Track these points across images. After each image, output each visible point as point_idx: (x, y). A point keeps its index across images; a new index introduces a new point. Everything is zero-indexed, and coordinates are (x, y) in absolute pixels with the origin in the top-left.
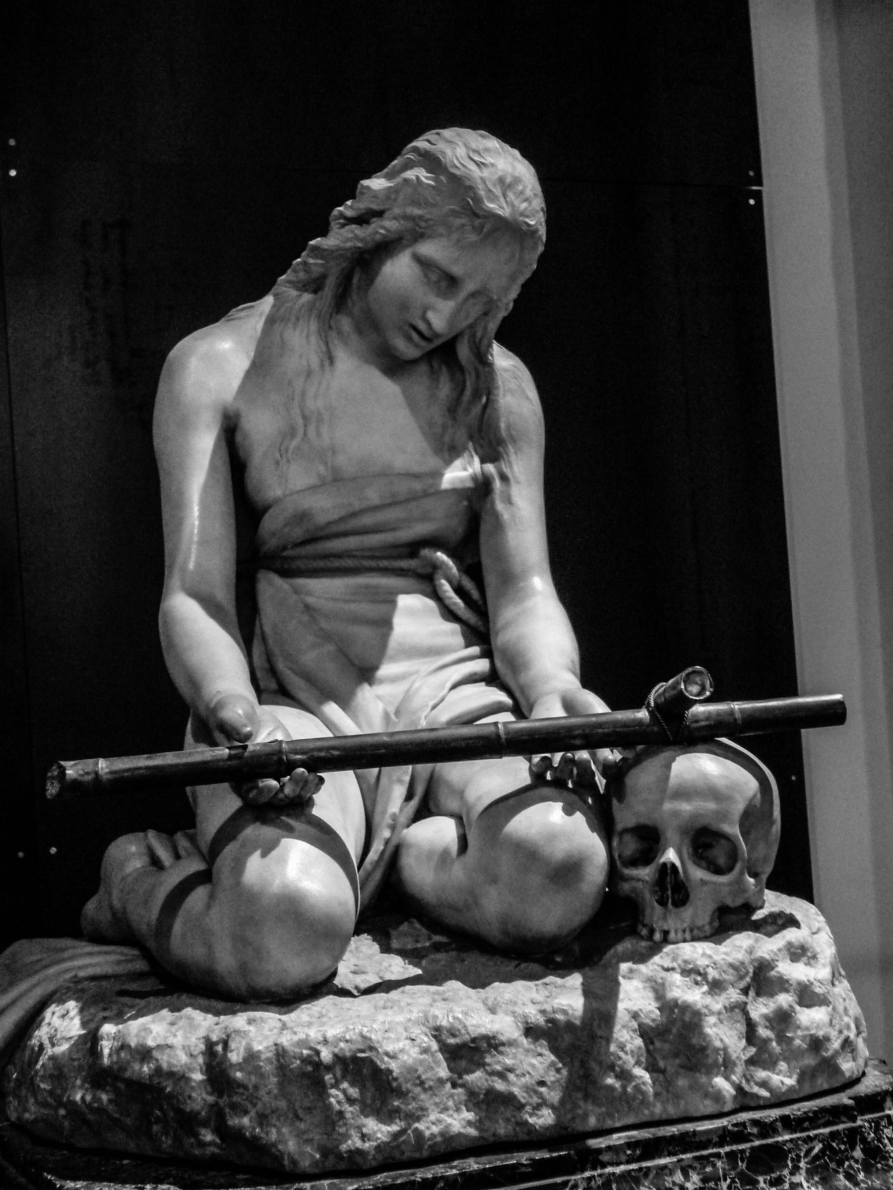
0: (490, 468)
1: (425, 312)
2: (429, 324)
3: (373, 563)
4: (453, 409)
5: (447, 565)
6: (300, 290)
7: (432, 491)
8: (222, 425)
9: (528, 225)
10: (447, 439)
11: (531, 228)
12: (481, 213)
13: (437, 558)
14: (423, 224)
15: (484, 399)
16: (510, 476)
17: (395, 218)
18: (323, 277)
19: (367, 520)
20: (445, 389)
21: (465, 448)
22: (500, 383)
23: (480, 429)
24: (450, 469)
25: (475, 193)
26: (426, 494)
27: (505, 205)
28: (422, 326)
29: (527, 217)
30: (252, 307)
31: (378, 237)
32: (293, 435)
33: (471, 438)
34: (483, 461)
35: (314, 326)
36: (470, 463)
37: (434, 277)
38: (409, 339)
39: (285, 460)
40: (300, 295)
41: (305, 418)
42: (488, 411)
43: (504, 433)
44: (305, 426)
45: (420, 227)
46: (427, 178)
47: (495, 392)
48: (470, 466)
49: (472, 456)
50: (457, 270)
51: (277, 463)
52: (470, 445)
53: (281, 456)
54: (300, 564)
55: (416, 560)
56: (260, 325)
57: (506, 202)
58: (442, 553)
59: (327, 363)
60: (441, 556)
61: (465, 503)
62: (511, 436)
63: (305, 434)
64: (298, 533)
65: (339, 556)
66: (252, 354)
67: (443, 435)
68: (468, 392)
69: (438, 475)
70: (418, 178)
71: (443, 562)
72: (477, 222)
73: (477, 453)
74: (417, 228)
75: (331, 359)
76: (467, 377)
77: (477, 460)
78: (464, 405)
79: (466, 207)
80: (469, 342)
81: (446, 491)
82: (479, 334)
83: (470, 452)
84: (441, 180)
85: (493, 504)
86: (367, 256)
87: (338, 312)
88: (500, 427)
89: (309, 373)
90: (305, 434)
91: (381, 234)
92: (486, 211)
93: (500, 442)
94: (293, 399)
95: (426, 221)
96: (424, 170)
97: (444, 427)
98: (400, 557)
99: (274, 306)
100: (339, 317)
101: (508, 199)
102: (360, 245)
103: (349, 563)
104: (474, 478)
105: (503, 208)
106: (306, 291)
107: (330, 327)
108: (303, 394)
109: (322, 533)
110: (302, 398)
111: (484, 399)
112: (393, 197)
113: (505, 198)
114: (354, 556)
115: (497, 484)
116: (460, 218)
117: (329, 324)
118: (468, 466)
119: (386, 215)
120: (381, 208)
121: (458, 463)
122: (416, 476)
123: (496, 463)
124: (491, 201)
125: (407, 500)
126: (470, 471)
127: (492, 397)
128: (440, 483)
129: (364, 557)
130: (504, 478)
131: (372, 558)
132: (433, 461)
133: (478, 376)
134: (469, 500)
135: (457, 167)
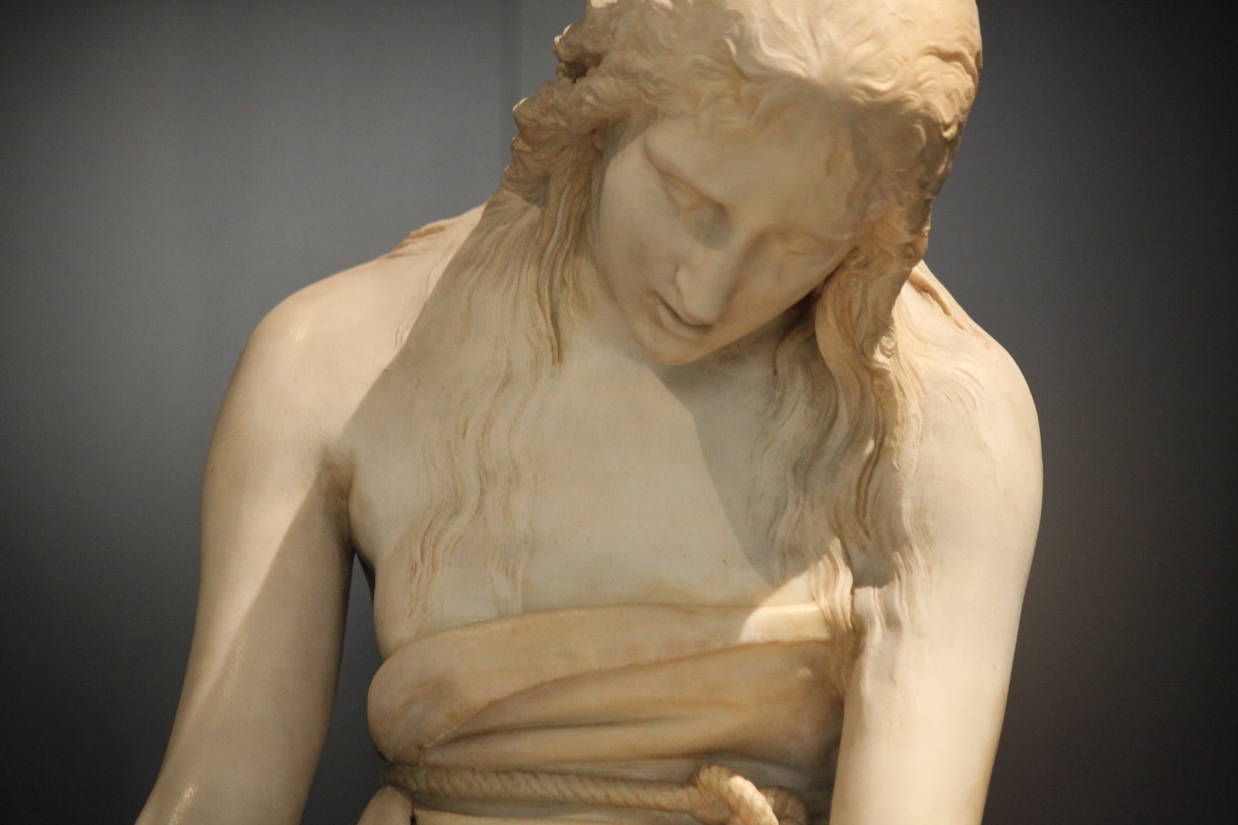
0: (870, 597)
1: (676, 270)
3: (596, 792)
5: (751, 810)
6: (527, 200)
7: (719, 645)
9: (870, 91)
11: (880, 99)
12: (749, 69)
13: (730, 791)
14: (652, 89)
15: (870, 446)
16: (904, 618)
18: (546, 178)
19: (589, 699)
21: (822, 551)
22: (914, 409)
23: (860, 510)
24: (778, 596)
25: (742, 27)
26: (705, 653)
27: (810, 52)
28: (673, 302)
29: (871, 74)
30: (442, 229)
32: (456, 512)
33: (839, 531)
34: (858, 583)
35: (529, 277)
36: (830, 584)
37: (684, 200)
39: (428, 561)
40: (525, 209)
41: (485, 476)
42: (878, 472)
43: (907, 523)
44: (483, 492)
47: (897, 431)
48: (827, 591)
49: (836, 569)
50: (715, 188)
51: (414, 569)
52: (835, 546)
53: (422, 554)
54: (460, 783)
55: (691, 790)
56: (437, 274)
57: (816, 45)
58: (746, 777)
59: (548, 357)
60: (743, 787)
61: (805, 673)
62: (925, 530)
63: (480, 506)
64: (438, 721)
65: (531, 772)
66: (406, 335)
67: (773, 522)
68: (842, 428)
69: (747, 606)
72: (745, 88)
73: (849, 562)
74: (643, 96)
75: (559, 351)
76: (841, 395)
77: (845, 578)
78: (827, 458)
79: (724, 58)
80: (840, 322)
81: (750, 646)
82: (856, 307)
88: (898, 512)
89: (508, 380)
90: (480, 506)
91: (589, 104)
92: (763, 67)
93: (898, 541)
94: (464, 433)
95: (657, 83)
97: (779, 507)
99: (478, 230)
101: (820, 40)
102: (563, 123)
103: (548, 788)
104: (831, 623)
105: (805, 59)
109: (493, 720)
110: (483, 435)
111: (870, 446)
112: (612, 26)
113: (813, 36)
114: (562, 774)
115: (876, 636)
117: (562, 271)
118: (822, 593)
121: (799, 584)
122: (687, 609)
123: (885, 588)
124: (776, 43)
125: (658, 664)
126: (824, 603)
129: (580, 776)
130: (892, 622)
131: (592, 778)
132: (745, 578)
133: (863, 398)
134: (812, 664)
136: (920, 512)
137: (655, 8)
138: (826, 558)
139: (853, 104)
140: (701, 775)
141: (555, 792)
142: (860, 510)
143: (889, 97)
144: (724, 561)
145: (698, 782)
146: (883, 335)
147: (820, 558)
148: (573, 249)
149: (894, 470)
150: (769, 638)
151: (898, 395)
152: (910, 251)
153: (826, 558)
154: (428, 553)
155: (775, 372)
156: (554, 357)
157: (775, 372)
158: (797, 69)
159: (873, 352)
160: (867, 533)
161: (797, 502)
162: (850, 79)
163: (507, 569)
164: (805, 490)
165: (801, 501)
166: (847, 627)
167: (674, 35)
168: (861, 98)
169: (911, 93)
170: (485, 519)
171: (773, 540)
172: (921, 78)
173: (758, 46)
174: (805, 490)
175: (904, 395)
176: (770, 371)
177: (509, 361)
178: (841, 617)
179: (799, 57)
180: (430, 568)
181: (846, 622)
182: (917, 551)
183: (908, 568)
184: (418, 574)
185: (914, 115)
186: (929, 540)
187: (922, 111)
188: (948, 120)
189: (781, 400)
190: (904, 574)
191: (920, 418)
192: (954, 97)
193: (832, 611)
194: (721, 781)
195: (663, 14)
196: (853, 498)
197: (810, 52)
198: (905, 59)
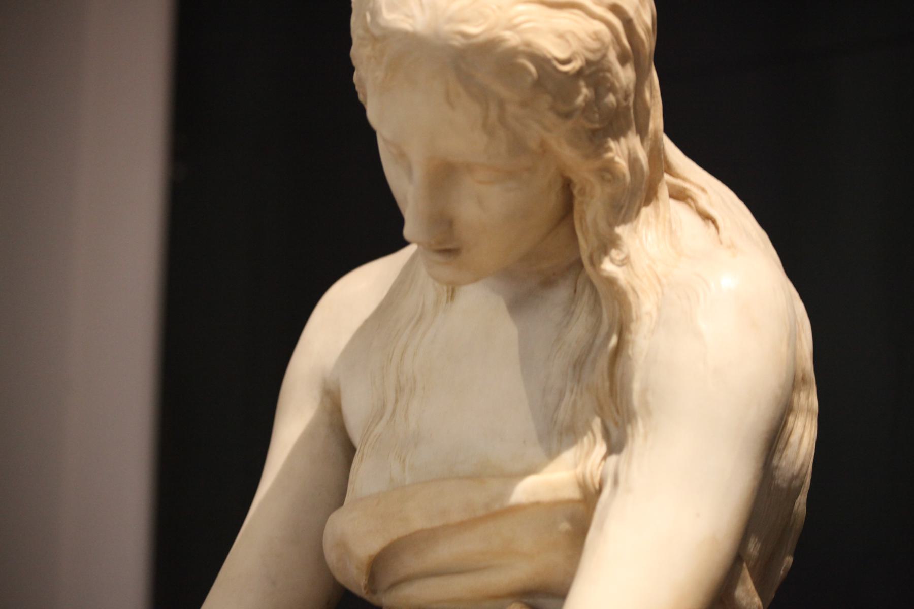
4: (579, 366)
8: (322, 402)
9: (465, 35)
11: (474, 40)
15: (614, 340)
20: (579, 329)
23: (613, 392)
24: (553, 466)
27: (417, 11)
33: (600, 411)
41: (399, 390)
44: (396, 401)
47: (633, 326)
52: (597, 423)
62: (646, 404)
63: (394, 411)
77: (601, 448)
83: (594, 436)
90: (394, 411)
105: (412, 17)
110: (401, 360)
121: (568, 456)
124: (393, 8)
126: (579, 470)
127: (628, 337)
128: (507, 493)
136: (644, 391)
138: (589, 434)
139: (452, 47)
142: (613, 392)
143: (482, 39)
146: (611, 248)
147: (585, 434)
149: (629, 358)
150: (532, 499)
151: (631, 297)
152: (608, 176)
153: (589, 434)
155: (575, 291)
156: (448, 297)
157: (575, 291)
158: (406, 25)
159: (601, 262)
161: (572, 391)
162: (447, 28)
163: (400, 458)
164: (579, 381)
165: (575, 390)
166: (595, 488)
168: (458, 42)
169: (507, 34)
172: (516, 21)
174: (579, 381)
175: (638, 297)
176: (572, 291)
178: (589, 481)
179: (408, 16)
181: (594, 485)
182: (640, 424)
183: (633, 436)
185: (514, 53)
186: (649, 413)
187: (522, 48)
188: (562, 55)
189: (573, 312)
191: (655, 314)
192: (569, 37)
193: (584, 476)
196: (607, 384)
197: (417, 11)
198: (499, 7)
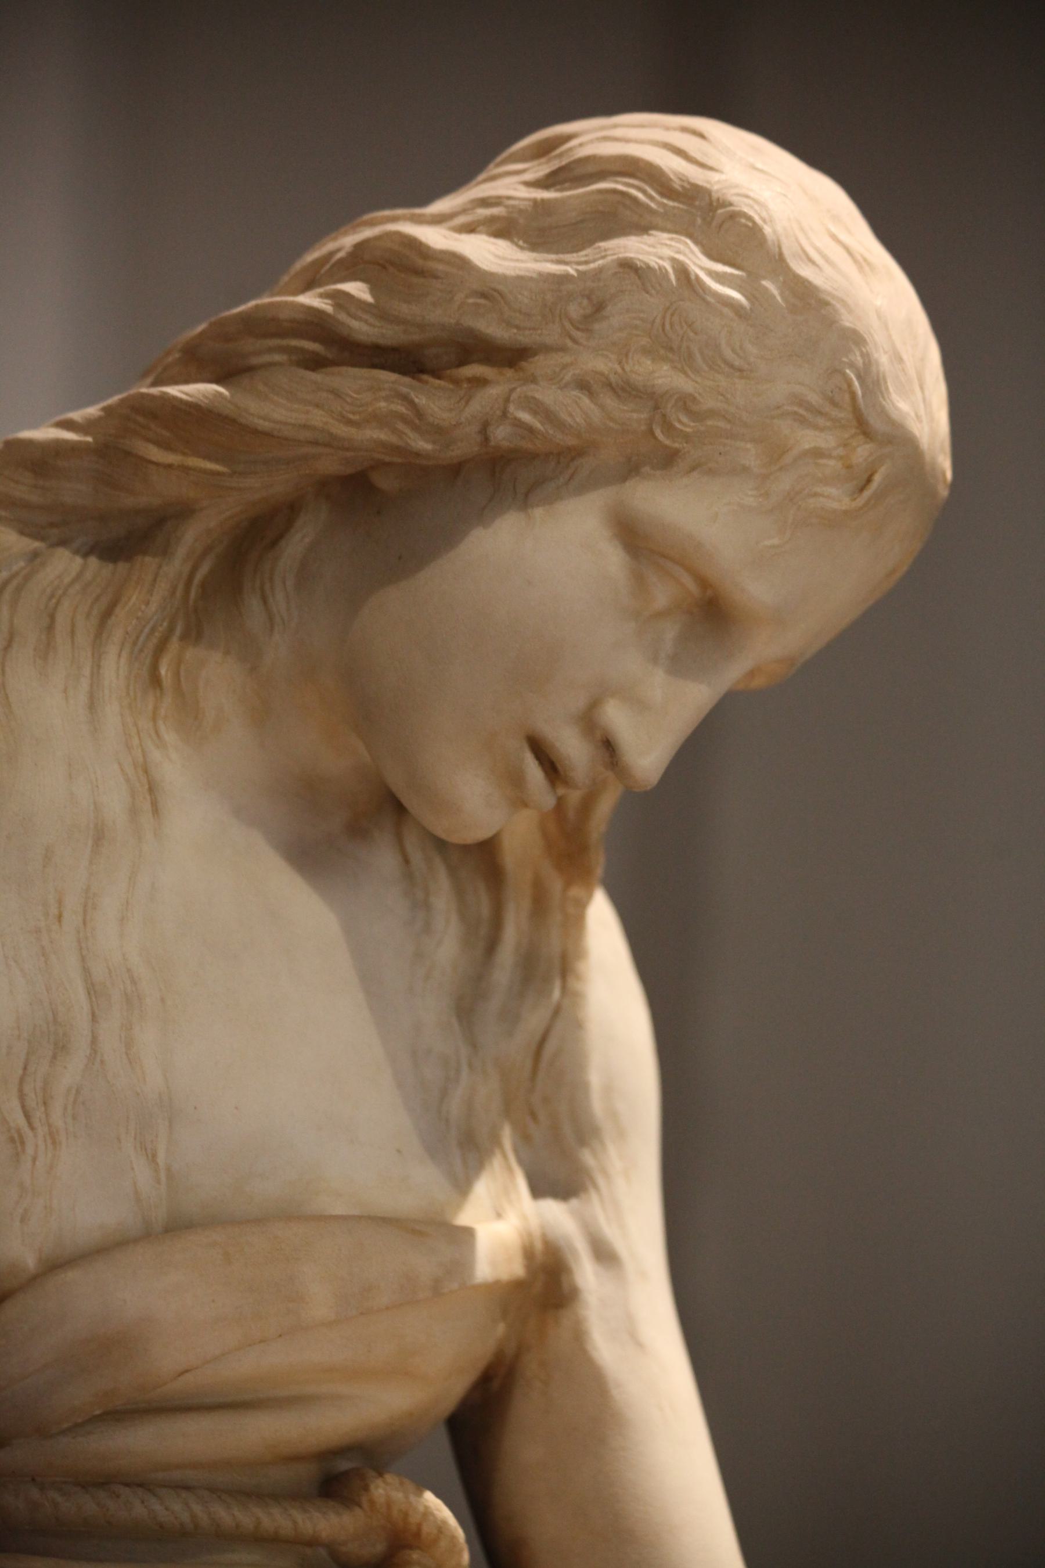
2: (608, 747)
7: (455, 1286)
10: (455, 1106)
12: (876, 423)
13: (427, 1513)
14: (684, 423)
17: (583, 385)
25: (866, 356)
31: (501, 434)
32: (61, 1048)
38: (515, 780)
39: (42, 1130)
41: (93, 990)
43: (597, 1105)
44: (94, 1018)
45: (669, 428)
46: (711, 273)
47: (581, 967)
49: (510, 1170)
53: (27, 1116)
55: (358, 1511)
62: (613, 1115)
63: (94, 1041)
70: (683, 272)
71: (441, 1528)
72: (862, 452)
83: (505, 1156)
84: (766, 289)
85: (579, 1336)
86: (384, 482)
87: (194, 634)
90: (94, 1041)
91: (518, 424)
94: (60, 917)
95: (696, 416)
96: (696, 249)
98: (294, 1496)
100: (191, 654)
102: (422, 445)
106: (63, 543)
107: (155, 680)
108: (89, 904)
110: (85, 923)
114: (187, 1488)
116: (816, 427)
119: (540, 364)
120: (525, 339)
121: (483, 1189)
123: (574, 1202)
135: (813, 263)
136: (608, 1090)
137: (709, 299)
140: (372, 1487)
141: (185, 1517)
144: (399, 1151)
145: (364, 1500)
148: (179, 630)
154: (38, 1114)
155: (407, 861)
157: (407, 861)
160: (533, 1115)
161: (470, 1066)
163: (146, 1149)
167: (752, 350)
170: (102, 1062)
171: (447, 1120)
173: (887, 389)
177: (95, 803)
180: (49, 1141)
182: (612, 1150)
184: (30, 1150)
186: (621, 1134)
190: (601, 1181)
194: (412, 1498)
195: (726, 310)
